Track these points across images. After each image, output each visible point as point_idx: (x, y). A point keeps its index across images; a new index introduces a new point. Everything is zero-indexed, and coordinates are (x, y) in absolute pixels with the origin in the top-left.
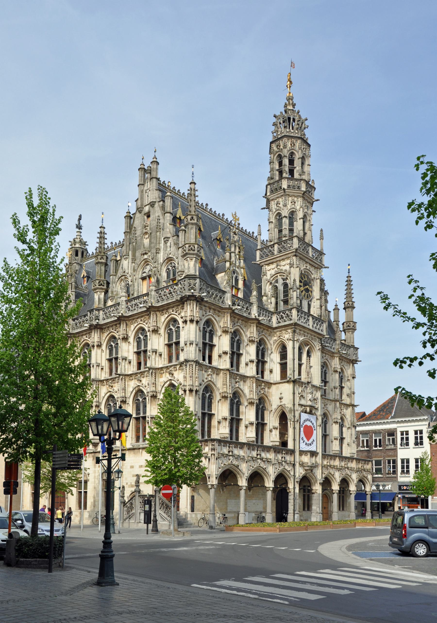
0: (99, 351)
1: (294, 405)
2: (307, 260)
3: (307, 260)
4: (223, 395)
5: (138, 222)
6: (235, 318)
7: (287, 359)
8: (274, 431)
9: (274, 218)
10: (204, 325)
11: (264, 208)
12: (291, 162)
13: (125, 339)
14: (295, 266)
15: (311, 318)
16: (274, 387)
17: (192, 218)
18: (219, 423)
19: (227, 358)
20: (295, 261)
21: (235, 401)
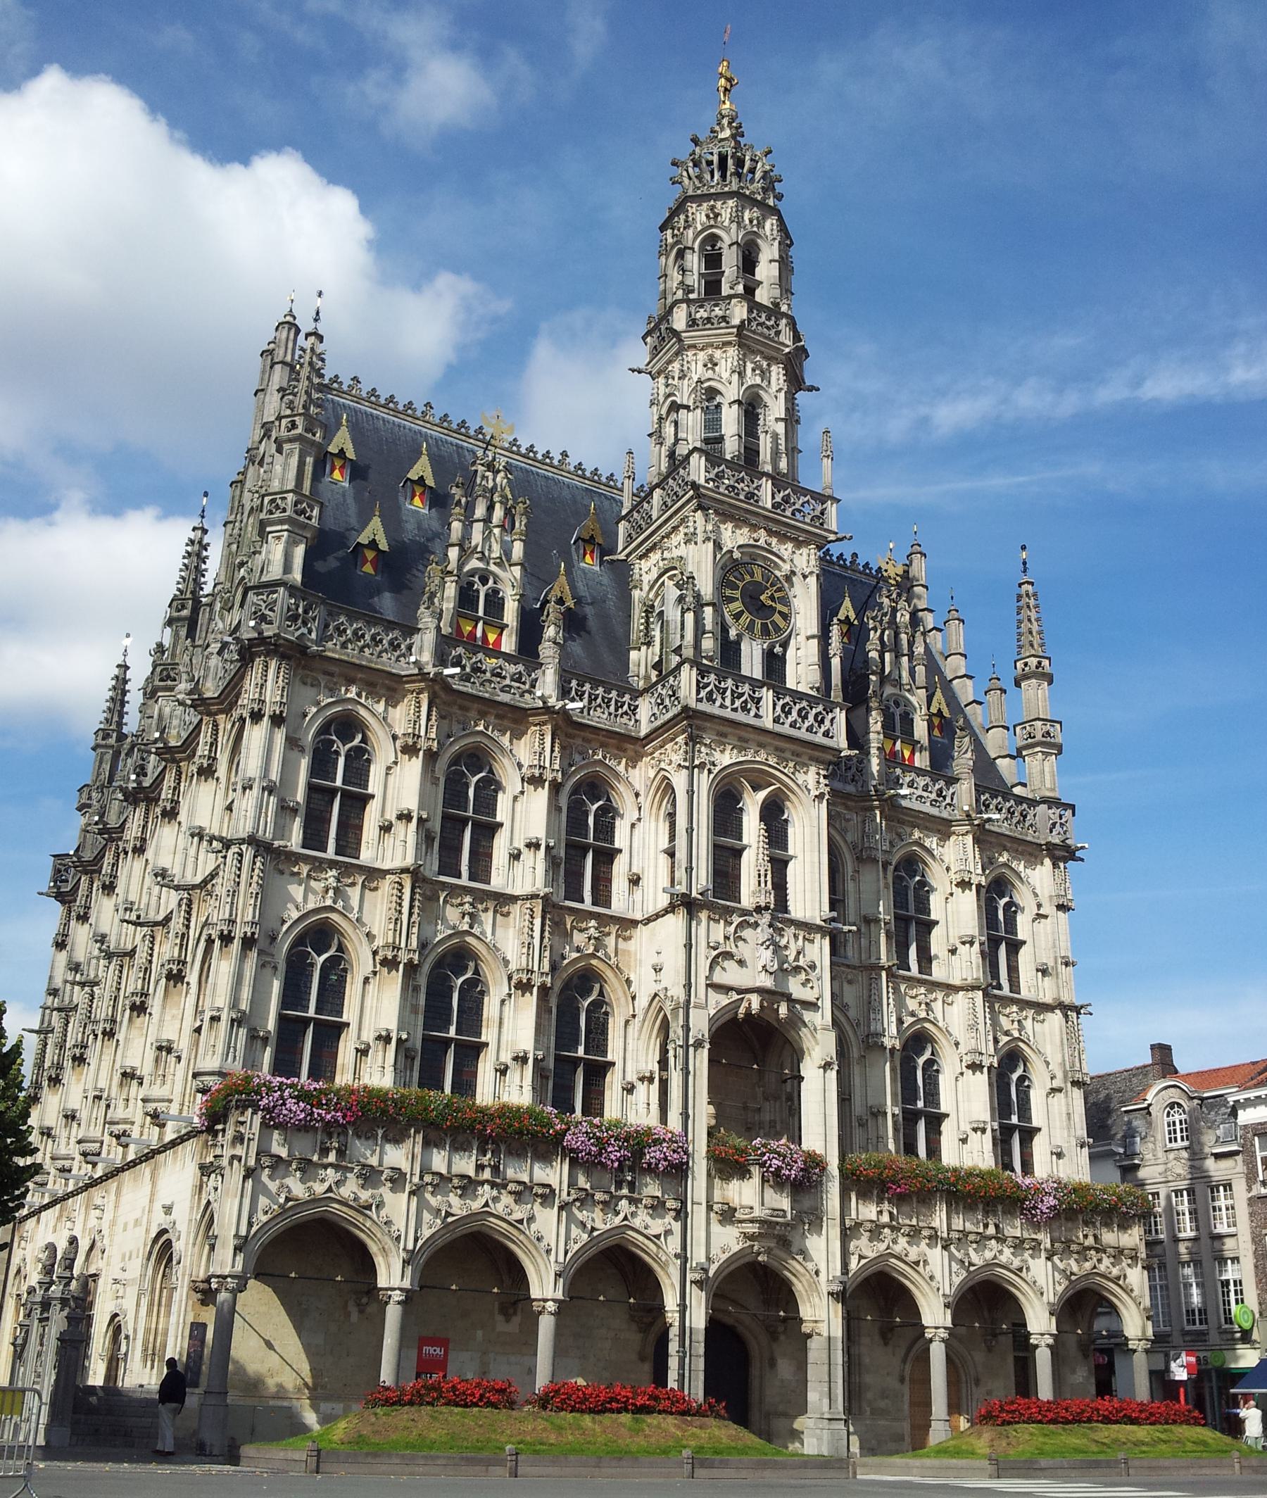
8: (641, 1088)
14: (700, 538)
16: (641, 933)
19: (408, 834)
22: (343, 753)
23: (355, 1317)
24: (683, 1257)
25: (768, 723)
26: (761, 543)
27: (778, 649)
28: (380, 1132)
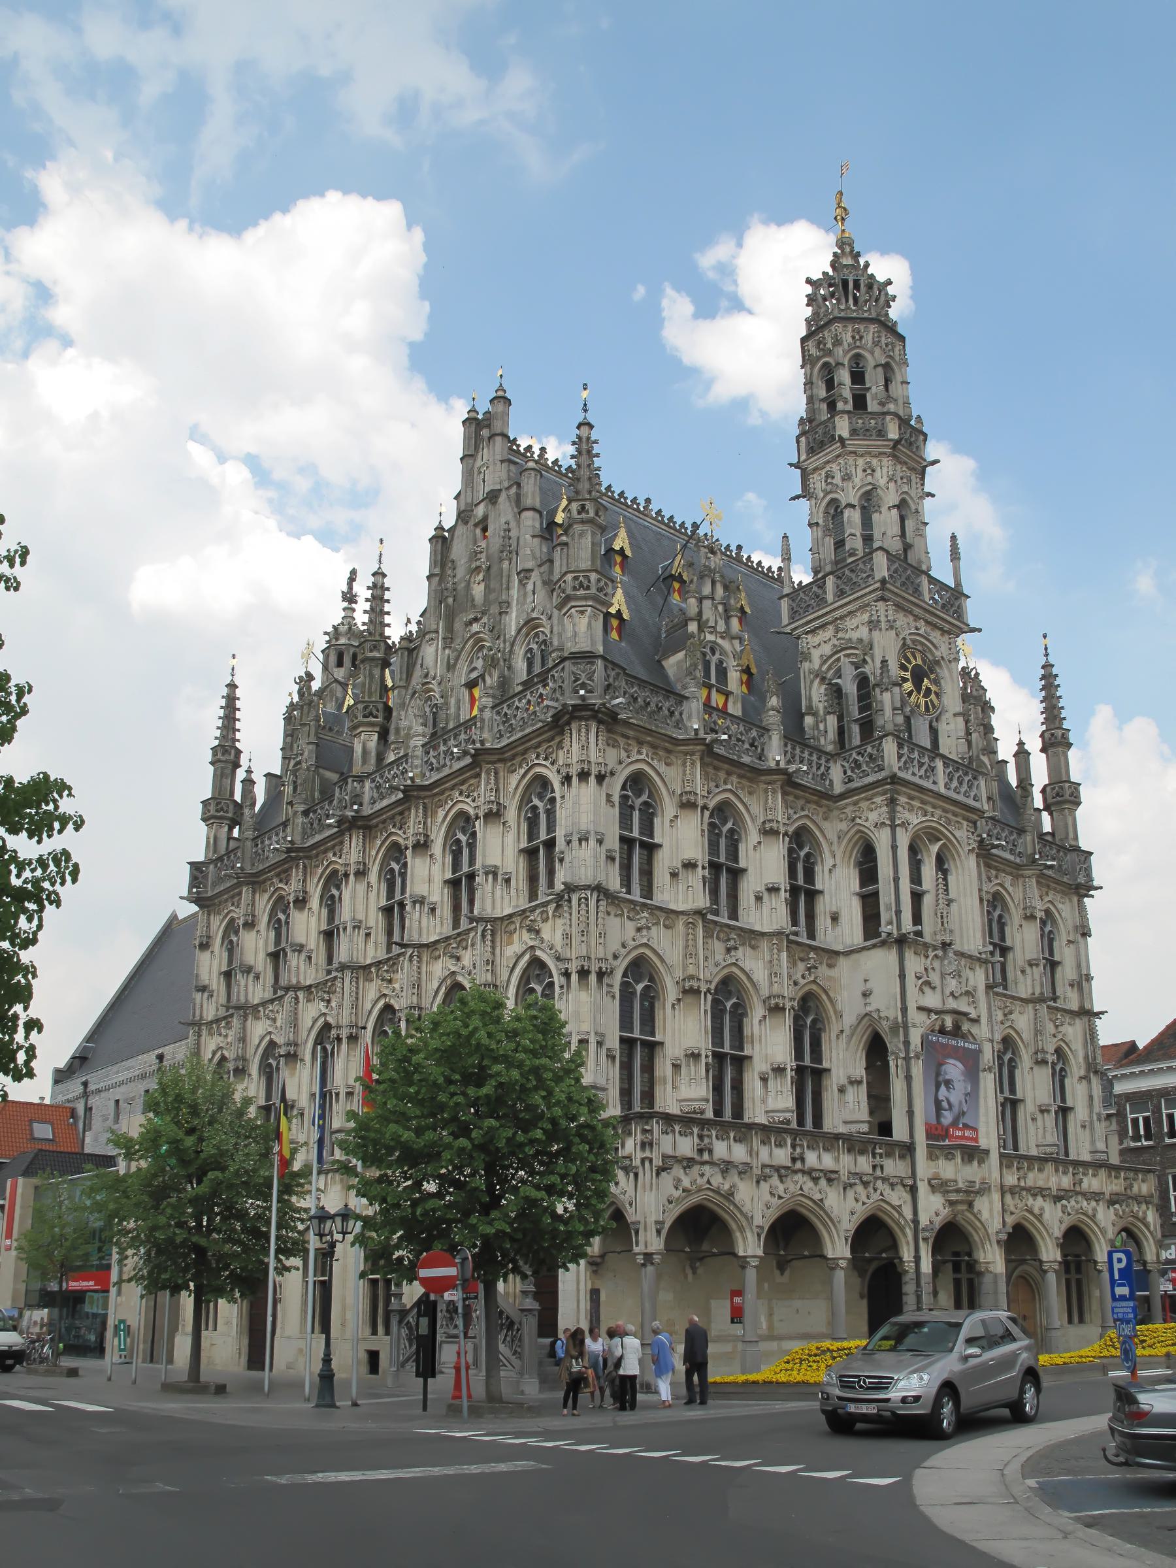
0: (361, 888)
1: (904, 1010)
2: (917, 611)
3: (917, 611)
4: (687, 985)
5: (459, 551)
6: (716, 768)
7: (877, 883)
9: (821, 514)
10: (624, 788)
11: (797, 497)
12: (858, 377)
13: (423, 846)
14: (883, 625)
15: (939, 764)
16: (843, 962)
17: (583, 507)
18: (676, 1067)
19: (696, 879)
20: (882, 613)
21: (727, 1003)
22: (637, 807)
23: (690, 1276)
24: (916, 1221)
25: (943, 791)
26: (921, 632)
27: (934, 724)
28: (732, 1135)
